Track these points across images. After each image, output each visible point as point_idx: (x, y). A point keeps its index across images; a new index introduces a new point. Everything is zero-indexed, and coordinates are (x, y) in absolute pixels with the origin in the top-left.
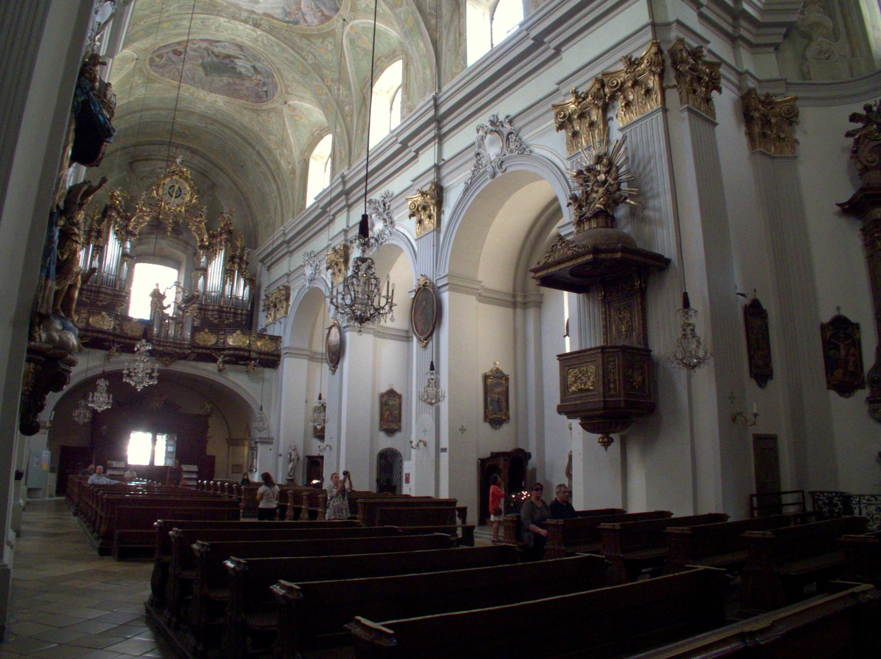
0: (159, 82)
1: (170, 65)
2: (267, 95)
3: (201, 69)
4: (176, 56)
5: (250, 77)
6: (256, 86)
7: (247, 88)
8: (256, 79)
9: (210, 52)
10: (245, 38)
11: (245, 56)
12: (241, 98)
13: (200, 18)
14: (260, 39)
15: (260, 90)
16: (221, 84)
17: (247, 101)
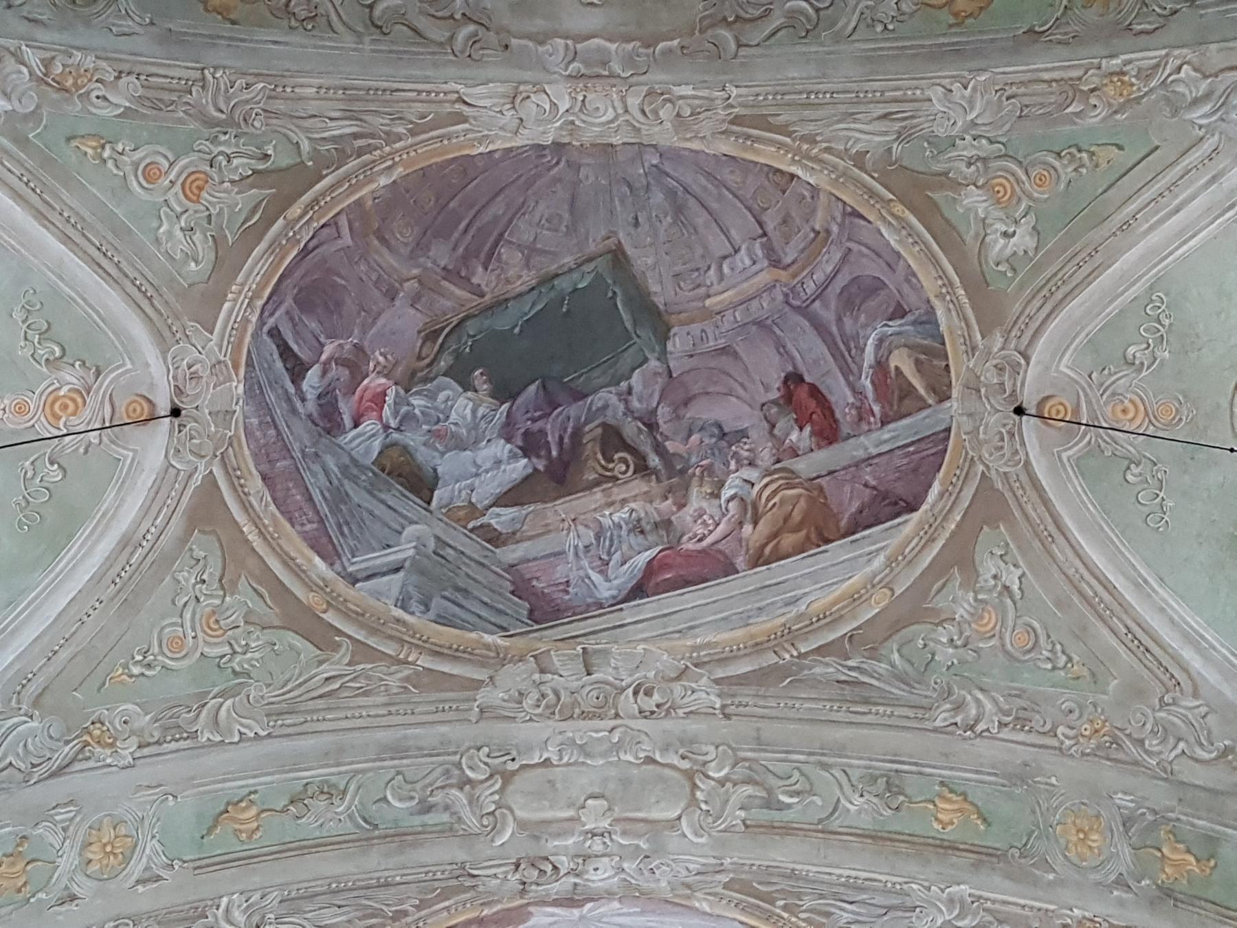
0: (859, 160)
1: (820, 294)
2: (285, 351)
3: (660, 291)
4: (807, 379)
5: (408, 383)
6: (358, 348)
7: (391, 295)
8: (379, 399)
9: (654, 461)
10: (551, 753)
11: (495, 538)
12: (396, 197)
13: (787, 830)
14: (488, 797)
15: (328, 350)
16: (524, 231)
17: (359, 203)
